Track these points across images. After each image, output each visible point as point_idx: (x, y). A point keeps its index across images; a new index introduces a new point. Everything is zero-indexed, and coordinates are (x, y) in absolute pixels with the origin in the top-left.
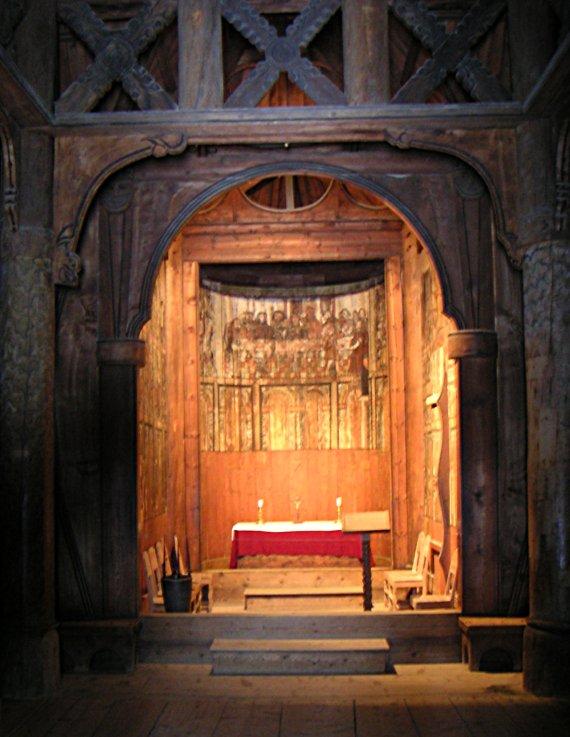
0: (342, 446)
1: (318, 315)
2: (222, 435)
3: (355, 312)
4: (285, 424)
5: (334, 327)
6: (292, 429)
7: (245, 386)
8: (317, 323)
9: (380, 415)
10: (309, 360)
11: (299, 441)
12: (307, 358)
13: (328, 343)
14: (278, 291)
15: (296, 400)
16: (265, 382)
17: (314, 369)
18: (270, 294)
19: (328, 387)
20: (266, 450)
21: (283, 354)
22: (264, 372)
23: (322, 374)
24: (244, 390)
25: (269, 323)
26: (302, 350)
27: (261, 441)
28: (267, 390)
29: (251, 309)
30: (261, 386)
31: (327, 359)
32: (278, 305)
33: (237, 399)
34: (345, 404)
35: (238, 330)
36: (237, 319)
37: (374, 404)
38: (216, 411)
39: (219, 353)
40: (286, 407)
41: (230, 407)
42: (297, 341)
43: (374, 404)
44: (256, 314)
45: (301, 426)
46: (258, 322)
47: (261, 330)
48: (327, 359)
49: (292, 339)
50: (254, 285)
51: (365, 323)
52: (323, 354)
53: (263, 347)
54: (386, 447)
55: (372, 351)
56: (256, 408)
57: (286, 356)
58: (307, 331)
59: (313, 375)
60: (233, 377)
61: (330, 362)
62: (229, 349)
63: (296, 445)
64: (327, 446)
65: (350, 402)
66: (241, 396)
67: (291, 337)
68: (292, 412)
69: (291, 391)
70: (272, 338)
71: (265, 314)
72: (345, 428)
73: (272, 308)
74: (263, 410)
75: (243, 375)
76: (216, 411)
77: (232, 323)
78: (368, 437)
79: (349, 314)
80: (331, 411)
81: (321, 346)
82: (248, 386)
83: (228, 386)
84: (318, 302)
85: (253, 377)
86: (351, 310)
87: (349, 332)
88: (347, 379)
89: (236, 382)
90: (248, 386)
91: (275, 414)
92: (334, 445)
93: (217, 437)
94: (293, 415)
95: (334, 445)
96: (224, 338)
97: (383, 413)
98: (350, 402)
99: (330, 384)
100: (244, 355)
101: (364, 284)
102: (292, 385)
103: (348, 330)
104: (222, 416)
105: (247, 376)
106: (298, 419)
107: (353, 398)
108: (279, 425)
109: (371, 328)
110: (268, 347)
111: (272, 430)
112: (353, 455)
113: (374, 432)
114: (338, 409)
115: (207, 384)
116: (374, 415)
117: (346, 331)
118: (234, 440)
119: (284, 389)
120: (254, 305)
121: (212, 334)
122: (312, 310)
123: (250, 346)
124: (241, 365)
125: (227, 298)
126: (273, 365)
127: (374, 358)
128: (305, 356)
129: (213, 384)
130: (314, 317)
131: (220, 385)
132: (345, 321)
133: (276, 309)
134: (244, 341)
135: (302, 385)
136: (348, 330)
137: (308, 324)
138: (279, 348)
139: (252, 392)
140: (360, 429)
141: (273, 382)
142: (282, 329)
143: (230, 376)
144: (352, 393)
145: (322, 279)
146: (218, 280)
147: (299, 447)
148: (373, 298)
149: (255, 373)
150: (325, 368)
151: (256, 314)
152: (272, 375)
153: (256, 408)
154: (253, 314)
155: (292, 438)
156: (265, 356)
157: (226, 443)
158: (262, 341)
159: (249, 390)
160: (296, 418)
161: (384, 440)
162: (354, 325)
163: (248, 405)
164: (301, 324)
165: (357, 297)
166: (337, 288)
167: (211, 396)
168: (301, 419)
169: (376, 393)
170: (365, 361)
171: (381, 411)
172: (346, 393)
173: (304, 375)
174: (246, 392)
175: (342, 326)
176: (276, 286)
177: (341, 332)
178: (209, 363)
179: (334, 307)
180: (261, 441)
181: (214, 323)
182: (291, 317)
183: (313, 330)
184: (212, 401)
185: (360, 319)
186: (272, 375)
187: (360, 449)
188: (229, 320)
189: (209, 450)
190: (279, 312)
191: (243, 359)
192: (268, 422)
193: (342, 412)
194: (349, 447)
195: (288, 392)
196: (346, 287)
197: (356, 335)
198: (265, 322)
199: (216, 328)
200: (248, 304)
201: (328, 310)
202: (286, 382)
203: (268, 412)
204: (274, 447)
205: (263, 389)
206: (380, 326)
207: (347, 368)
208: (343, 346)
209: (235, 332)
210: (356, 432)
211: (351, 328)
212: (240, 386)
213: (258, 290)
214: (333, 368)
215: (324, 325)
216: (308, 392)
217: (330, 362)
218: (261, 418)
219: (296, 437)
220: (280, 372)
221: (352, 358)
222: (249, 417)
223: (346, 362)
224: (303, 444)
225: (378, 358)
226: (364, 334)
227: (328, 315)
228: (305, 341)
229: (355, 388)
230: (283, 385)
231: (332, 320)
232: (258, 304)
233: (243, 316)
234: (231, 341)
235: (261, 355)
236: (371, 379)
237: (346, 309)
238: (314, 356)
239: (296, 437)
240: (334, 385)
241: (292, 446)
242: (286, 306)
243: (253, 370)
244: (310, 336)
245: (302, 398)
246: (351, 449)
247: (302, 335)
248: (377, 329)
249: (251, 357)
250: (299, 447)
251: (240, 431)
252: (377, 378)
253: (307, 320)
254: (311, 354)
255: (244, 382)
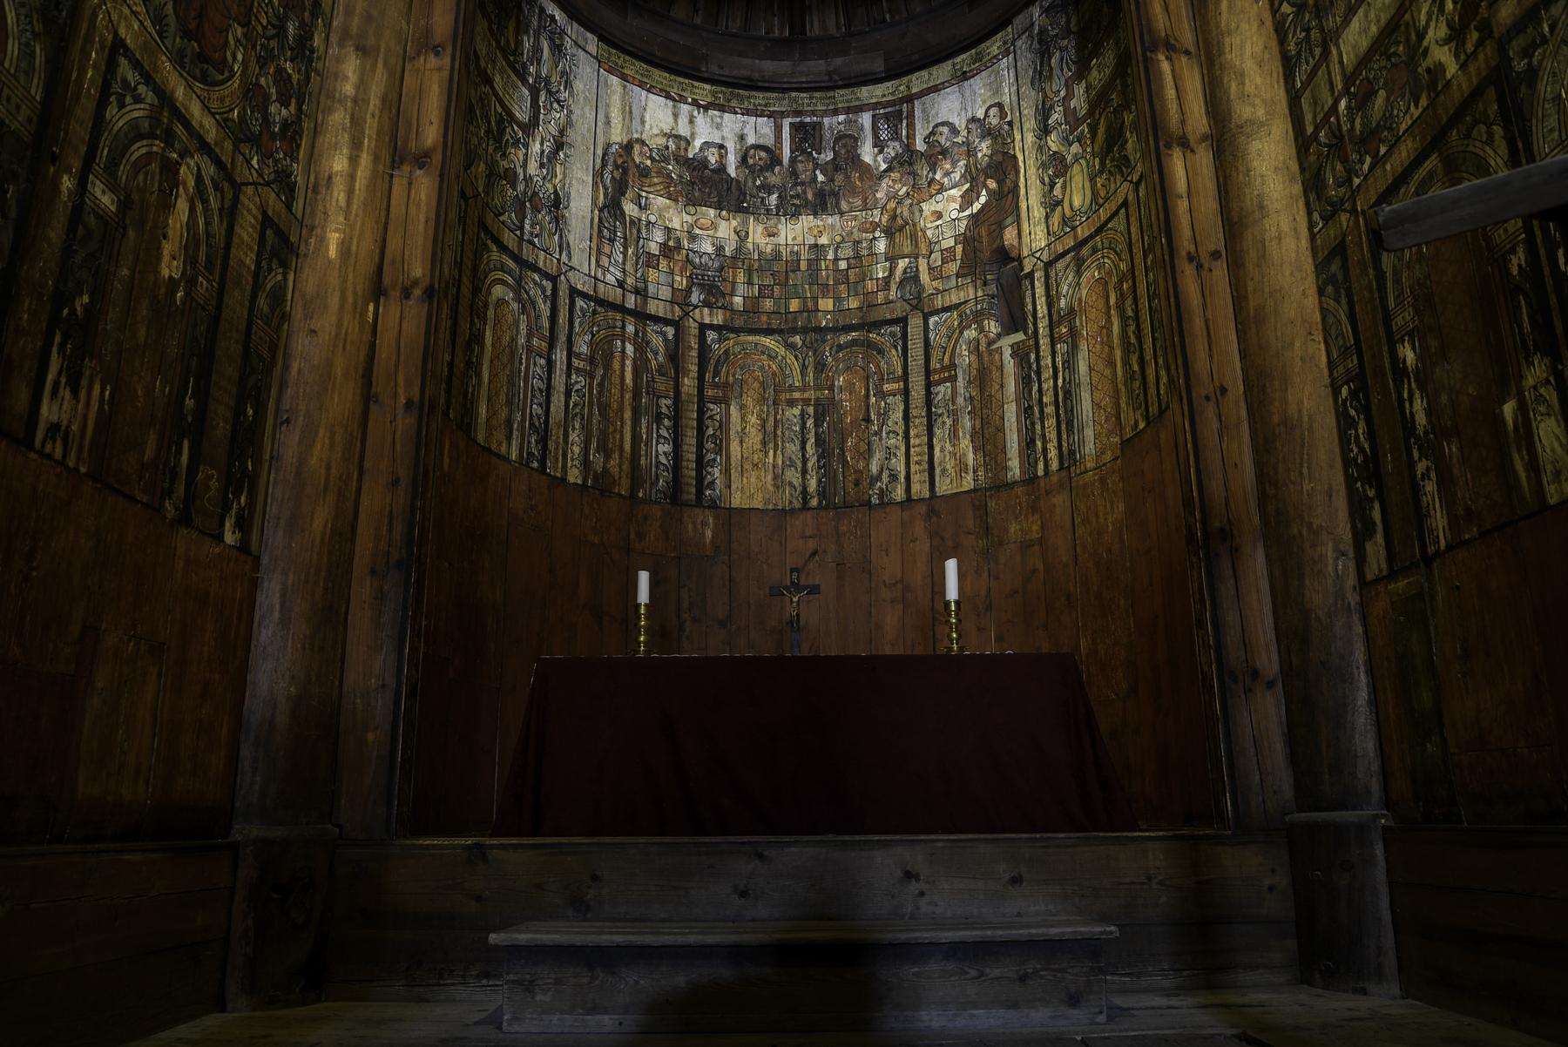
0: (944, 487)
1: (867, 153)
2: (574, 436)
3: (974, 120)
4: (770, 438)
5: (914, 174)
6: (793, 448)
7: (656, 319)
8: (865, 170)
9: (1070, 364)
10: (843, 265)
11: (813, 484)
12: (836, 260)
13: (894, 217)
14: (759, 98)
15: (804, 368)
16: (719, 318)
17: (855, 288)
18: (734, 103)
19: (897, 329)
20: (713, 505)
21: (768, 250)
22: (715, 293)
23: (881, 297)
24: (652, 328)
25: (732, 171)
26: (824, 240)
27: (700, 478)
28: (720, 341)
29: (683, 130)
30: (703, 327)
31: (892, 259)
32: (758, 130)
33: (630, 349)
34: (953, 366)
35: (644, 173)
36: (643, 143)
37: (1044, 342)
38: (560, 356)
39: (581, 204)
40: (776, 392)
41: (608, 366)
42: (807, 221)
43: (1044, 342)
44: (698, 143)
45: (819, 442)
46: (698, 165)
47: (704, 183)
48: (892, 259)
49: (795, 215)
50: (693, 74)
51: (999, 137)
52: (881, 246)
53: (714, 226)
54: (1100, 453)
55: (1032, 199)
56: (689, 384)
57: (777, 255)
58: (835, 194)
59: (854, 304)
60: (621, 284)
61: (902, 264)
62: (612, 207)
63: (804, 491)
64: (899, 493)
65: (965, 357)
66: (642, 345)
67: (791, 209)
68: (791, 403)
69: (791, 347)
70: (739, 210)
71: (721, 147)
72: (954, 435)
73: (742, 138)
74: (710, 393)
75: (651, 289)
76: (560, 356)
77: (628, 147)
78: (1028, 444)
79: (954, 131)
80: (906, 393)
81: (876, 226)
82: (667, 322)
83: (600, 302)
84: (866, 119)
85: (680, 299)
86: (960, 122)
87: (957, 176)
88: (954, 298)
89: (631, 301)
90: (667, 322)
91: (742, 407)
92: (920, 489)
93: (556, 433)
94: (796, 411)
95: (920, 489)
96: (598, 175)
97: (1083, 346)
98: (965, 357)
99: (903, 321)
100: (659, 236)
101: (994, 46)
102: (794, 331)
103: (953, 173)
104: (579, 381)
105: (665, 293)
106: (810, 423)
107: (975, 347)
108: (754, 437)
109: (1024, 144)
110: (726, 230)
111: (735, 447)
112: (981, 510)
113: (1051, 422)
114: (929, 385)
115: (536, 269)
116: (1047, 374)
117: (947, 174)
118: (613, 463)
119: (768, 341)
120: (691, 122)
121: (559, 146)
122: (848, 141)
123: (677, 219)
124: (651, 261)
125: (614, 80)
126: (741, 277)
127: (1038, 213)
128: (830, 256)
129: (554, 279)
130: (855, 160)
131: (574, 292)
132: (944, 152)
133: (751, 140)
134: (661, 201)
135: (818, 330)
136: (953, 173)
137: (839, 178)
138: (757, 234)
139: (676, 335)
140: (1001, 429)
141: (738, 323)
142: (769, 189)
143: (610, 279)
144: (971, 333)
145: (879, 66)
146: (589, 26)
147: (814, 502)
148: (1026, 60)
149: (688, 291)
150: (887, 281)
151: (698, 143)
152: (738, 300)
153: (689, 384)
154: (688, 143)
155: (793, 476)
156: (719, 250)
157: (586, 464)
158: (712, 212)
159: (670, 331)
160: (803, 415)
161: (1089, 433)
162: (971, 152)
163: (661, 370)
164: (821, 178)
165: (979, 86)
166: (918, 81)
167: (544, 308)
168: (817, 425)
169: (1050, 306)
170: (1009, 235)
171: (1074, 347)
172: (954, 335)
173: (826, 304)
174: (657, 339)
175: (933, 169)
176: (752, 85)
177: (931, 182)
178: (544, 216)
179: (911, 126)
180: (700, 478)
181: (569, 123)
182: (793, 160)
183: (853, 192)
184: (546, 324)
185: (988, 133)
186: (738, 300)
187: (999, 486)
188: (617, 136)
189: (524, 462)
190: (757, 147)
191: (654, 248)
192: (724, 426)
193: (942, 391)
194: (968, 483)
195: (782, 351)
196: (942, 72)
197: (974, 179)
198: (722, 169)
199: (572, 136)
200: (676, 116)
201: (896, 136)
202: (775, 324)
203: (724, 401)
204: (736, 502)
205: (711, 336)
206: (1056, 116)
207: (953, 267)
208: (939, 215)
209: (632, 171)
210: (988, 440)
211: (961, 163)
212: (642, 316)
213: (704, 91)
214: (911, 278)
215: (881, 177)
216: (840, 348)
217: (902, 264)
218: (701, 412)
219: (804, 472)
220: (761, 295)
221: (968, 240)
222: (665, 403)
223: (948, 256)
224: (822, 494)
225: (1052, 205)
226: (1003, 166)
227: (893, 149)
228: (830, 220)
229: (978, 317)
230: (768, 332)
231: (906, 161)
232: (700, 119)
233: (662, 141)
234: (621, 188)
235: (710, 250)
236: (1031, 275)
237: (943, 124)
238: (858, 257)
239: (804, 472)
240: (915, 323)
241: (787, 498)
242: (778, 130)
243: (681, 281)
244: (844, 206)
245: (820, 366)
246: (975, 490)
247: (822, 203)
248: (1044, 130)
249: (679, 247)
250: (814, 502)
251: (636, 438)
252: (1048, 265)
253: (835, 167)
254: (847, 252)
255: (654, 308)
